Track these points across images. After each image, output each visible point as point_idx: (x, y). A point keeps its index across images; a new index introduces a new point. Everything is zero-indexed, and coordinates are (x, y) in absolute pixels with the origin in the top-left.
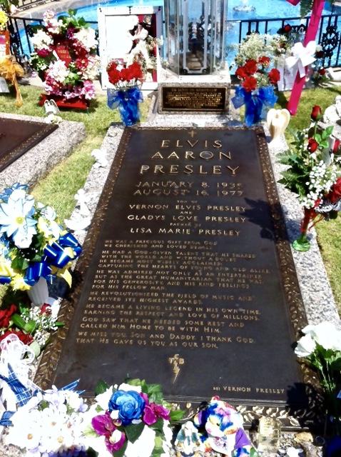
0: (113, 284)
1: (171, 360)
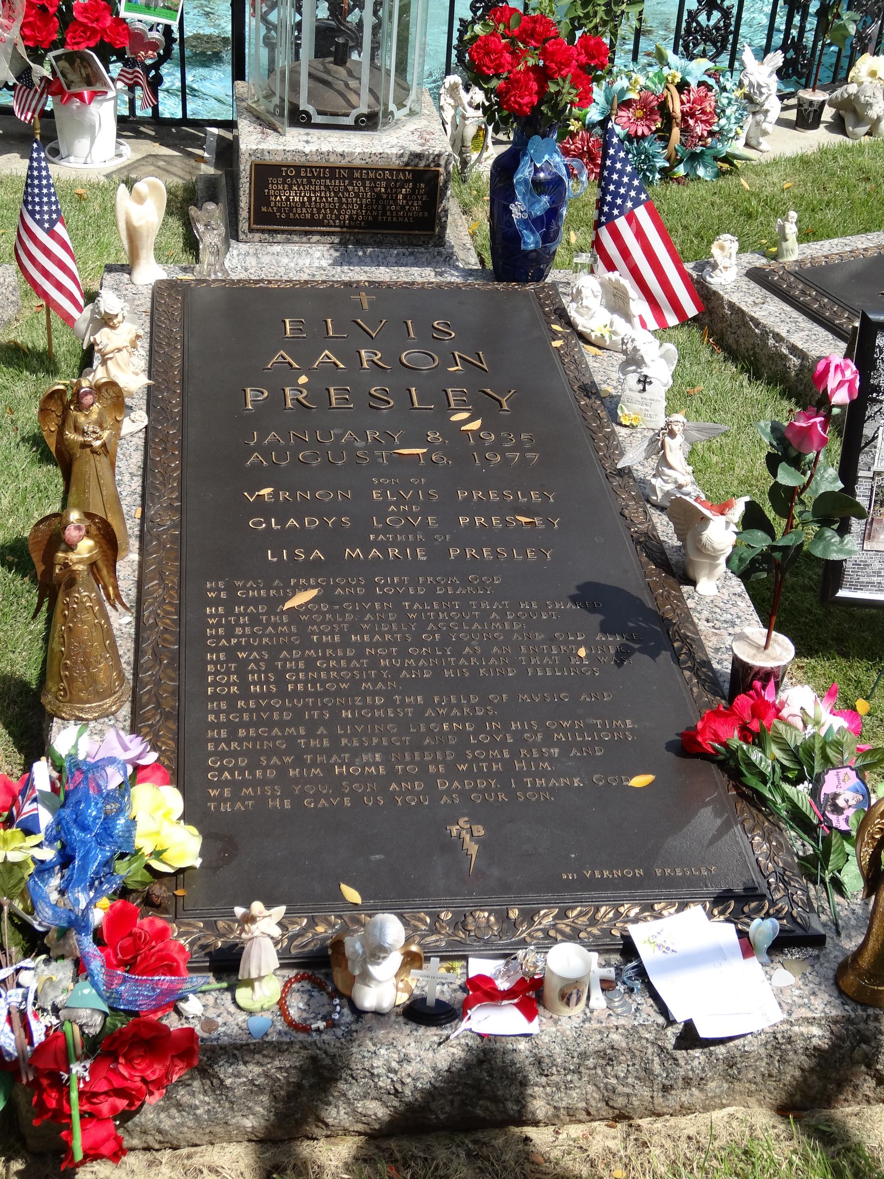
1: (454, 830)
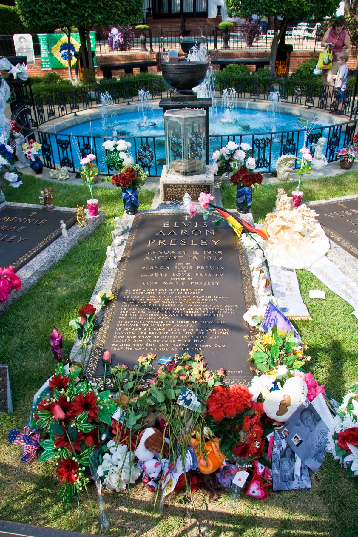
0: (132, 317)
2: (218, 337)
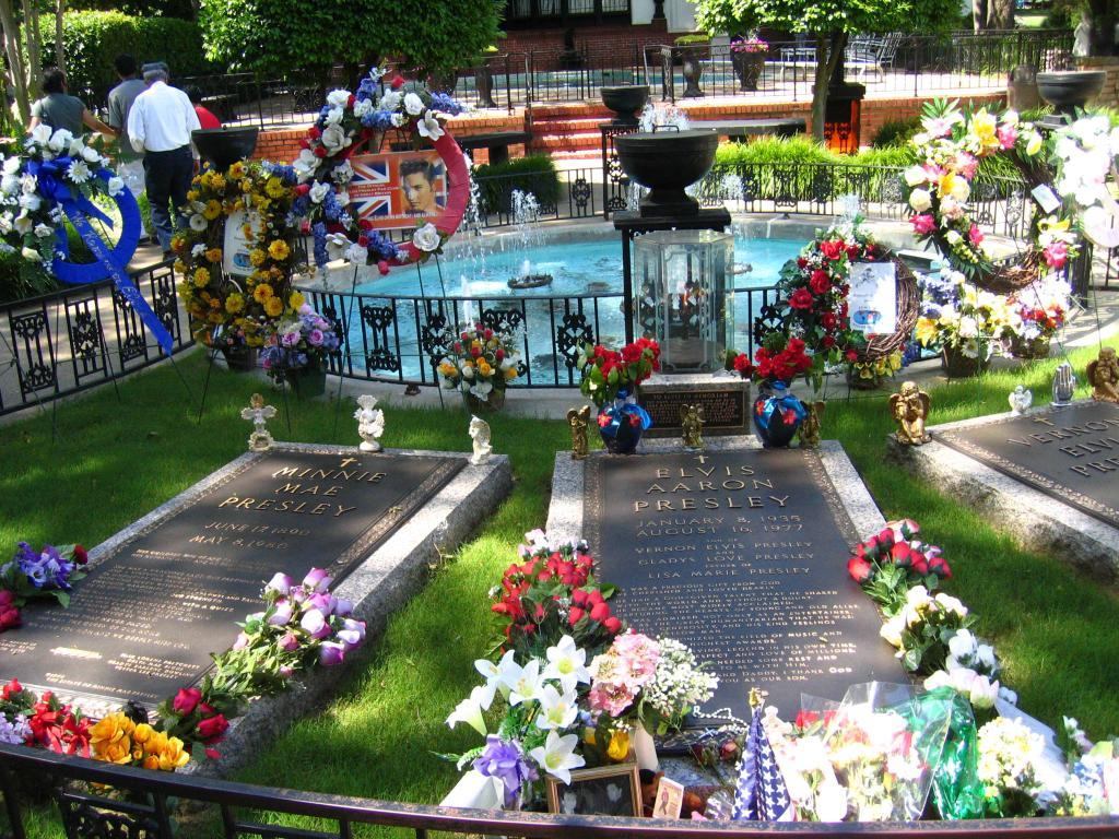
2: (834, 657)
